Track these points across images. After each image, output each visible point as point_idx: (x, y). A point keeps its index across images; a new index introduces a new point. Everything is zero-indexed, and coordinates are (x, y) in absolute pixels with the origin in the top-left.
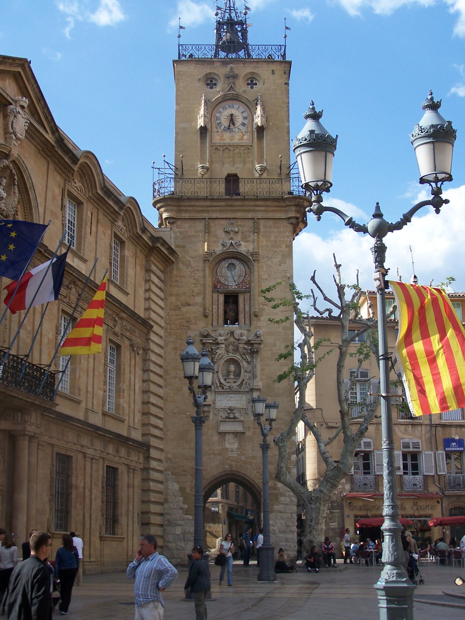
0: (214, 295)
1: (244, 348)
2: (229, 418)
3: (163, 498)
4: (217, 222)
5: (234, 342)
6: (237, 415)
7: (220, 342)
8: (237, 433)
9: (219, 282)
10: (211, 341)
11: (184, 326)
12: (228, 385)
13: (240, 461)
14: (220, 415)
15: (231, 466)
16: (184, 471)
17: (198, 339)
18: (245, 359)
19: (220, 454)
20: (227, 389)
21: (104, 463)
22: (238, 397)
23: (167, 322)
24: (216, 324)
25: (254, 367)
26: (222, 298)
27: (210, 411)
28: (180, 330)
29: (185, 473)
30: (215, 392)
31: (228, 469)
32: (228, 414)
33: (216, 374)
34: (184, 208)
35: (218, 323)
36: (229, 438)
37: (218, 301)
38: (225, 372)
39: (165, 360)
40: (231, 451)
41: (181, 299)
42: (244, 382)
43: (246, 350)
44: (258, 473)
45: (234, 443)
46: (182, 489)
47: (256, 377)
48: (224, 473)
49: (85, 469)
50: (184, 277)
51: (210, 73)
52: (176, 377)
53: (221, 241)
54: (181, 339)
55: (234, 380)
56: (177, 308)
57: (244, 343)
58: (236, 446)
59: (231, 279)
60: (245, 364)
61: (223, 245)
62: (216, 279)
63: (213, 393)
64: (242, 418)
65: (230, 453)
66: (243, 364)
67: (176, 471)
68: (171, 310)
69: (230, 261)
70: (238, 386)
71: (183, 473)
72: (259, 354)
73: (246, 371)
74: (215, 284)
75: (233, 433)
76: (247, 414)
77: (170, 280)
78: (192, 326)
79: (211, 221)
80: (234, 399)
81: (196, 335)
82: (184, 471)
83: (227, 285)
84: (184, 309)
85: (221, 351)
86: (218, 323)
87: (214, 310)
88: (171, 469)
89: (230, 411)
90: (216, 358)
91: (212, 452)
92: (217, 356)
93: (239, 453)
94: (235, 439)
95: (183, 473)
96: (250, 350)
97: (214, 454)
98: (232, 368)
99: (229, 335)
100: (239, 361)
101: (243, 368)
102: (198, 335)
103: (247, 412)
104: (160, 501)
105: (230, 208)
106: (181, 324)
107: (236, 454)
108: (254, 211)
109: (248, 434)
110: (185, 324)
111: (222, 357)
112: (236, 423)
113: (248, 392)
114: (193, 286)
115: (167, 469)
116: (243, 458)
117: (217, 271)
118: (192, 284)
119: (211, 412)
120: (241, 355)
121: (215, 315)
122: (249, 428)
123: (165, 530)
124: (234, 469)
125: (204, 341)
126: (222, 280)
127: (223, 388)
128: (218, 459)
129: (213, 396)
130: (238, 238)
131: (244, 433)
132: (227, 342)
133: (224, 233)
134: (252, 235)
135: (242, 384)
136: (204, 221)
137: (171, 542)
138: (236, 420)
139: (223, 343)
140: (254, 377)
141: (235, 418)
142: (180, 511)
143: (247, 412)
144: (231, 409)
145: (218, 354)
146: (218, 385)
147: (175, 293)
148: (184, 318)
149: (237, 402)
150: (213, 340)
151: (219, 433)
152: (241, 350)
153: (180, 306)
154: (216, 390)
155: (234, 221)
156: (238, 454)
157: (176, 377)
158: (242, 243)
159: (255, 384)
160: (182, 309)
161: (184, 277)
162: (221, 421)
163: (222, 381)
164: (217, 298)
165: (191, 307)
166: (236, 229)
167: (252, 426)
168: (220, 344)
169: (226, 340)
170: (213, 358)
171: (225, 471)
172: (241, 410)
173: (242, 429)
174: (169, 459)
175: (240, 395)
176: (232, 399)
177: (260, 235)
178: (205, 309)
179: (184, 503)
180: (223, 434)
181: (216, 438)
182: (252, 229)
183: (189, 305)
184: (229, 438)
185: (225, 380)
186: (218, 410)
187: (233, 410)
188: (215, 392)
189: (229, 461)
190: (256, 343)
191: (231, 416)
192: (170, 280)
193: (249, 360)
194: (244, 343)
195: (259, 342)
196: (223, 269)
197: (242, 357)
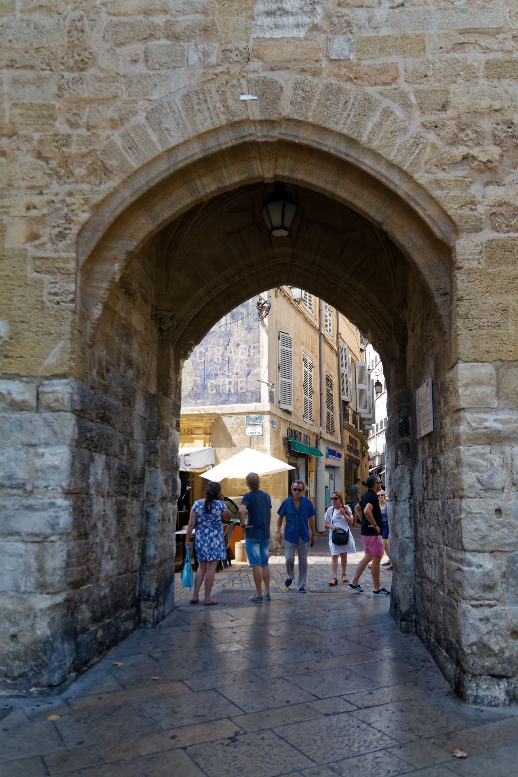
13: (324, 64)
31: (255, 114)
40: (269, 13)
65: (268, 21)
91: (159, 20)
128: (193, 58)
156: (315, 27)
171: (234, 125)
189: (255, 64)
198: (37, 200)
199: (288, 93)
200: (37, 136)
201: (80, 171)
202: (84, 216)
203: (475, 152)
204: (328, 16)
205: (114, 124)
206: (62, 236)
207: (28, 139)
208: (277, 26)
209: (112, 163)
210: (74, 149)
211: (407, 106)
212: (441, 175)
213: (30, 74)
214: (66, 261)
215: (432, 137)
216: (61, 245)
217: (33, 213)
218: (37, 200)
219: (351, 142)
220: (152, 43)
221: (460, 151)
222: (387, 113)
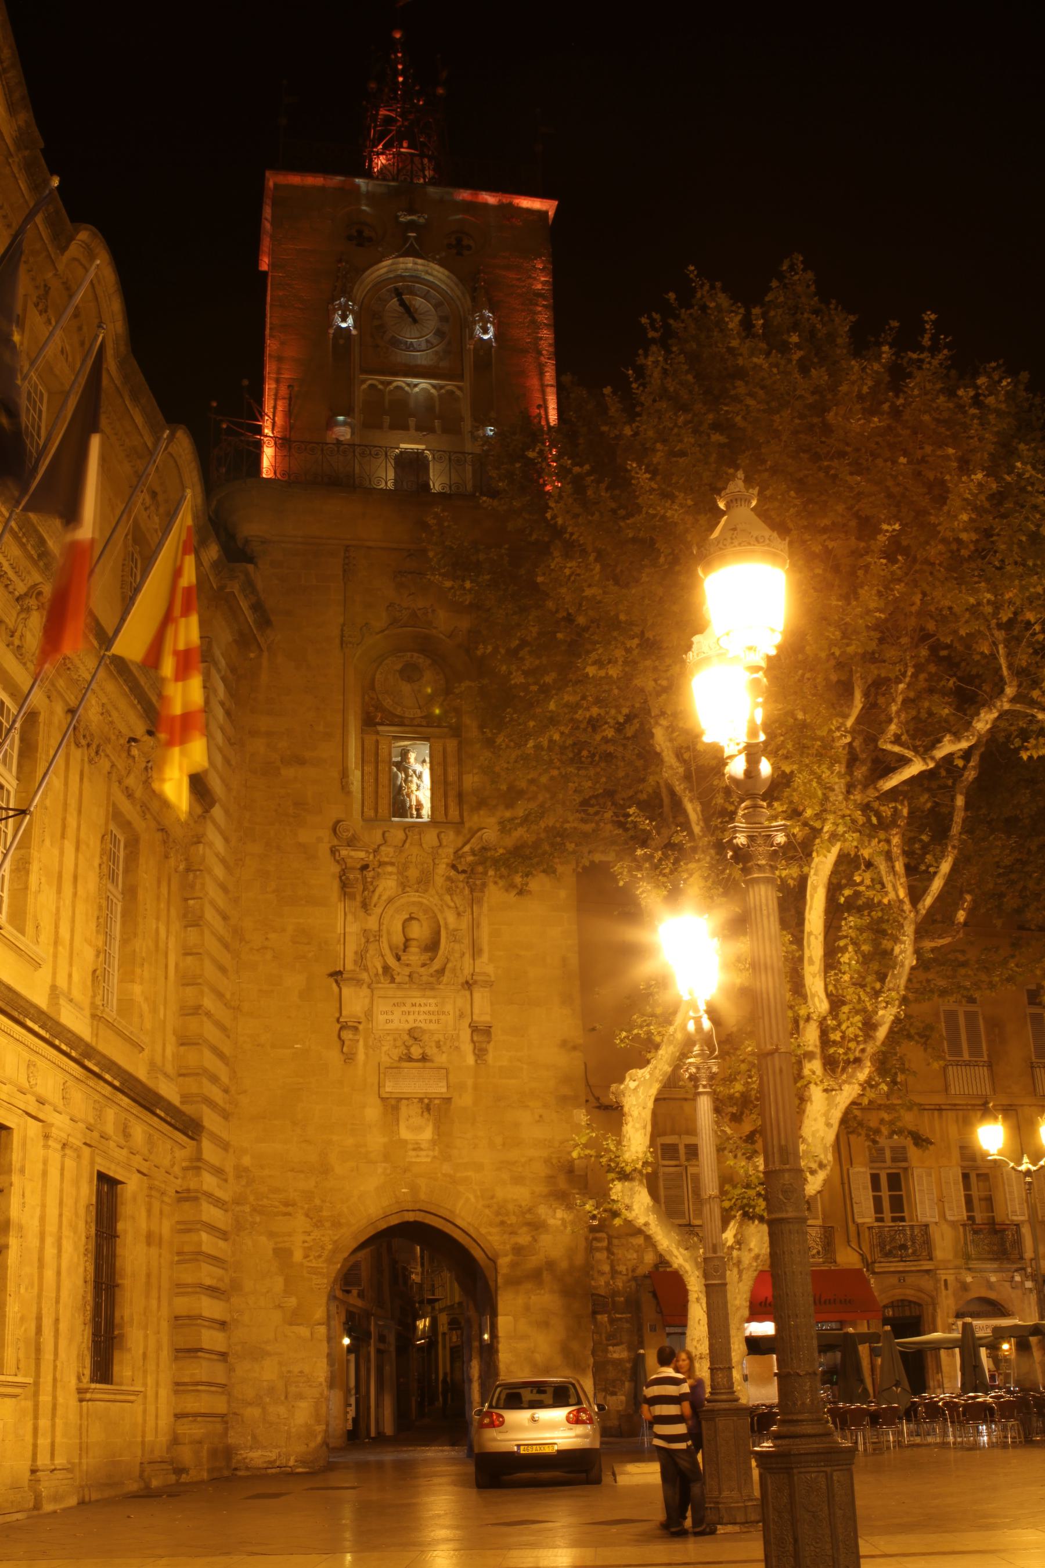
2: (410, 1059)
3: (227, 1280)
6: (432, 1051)
7: (386, 859)
15: (414, 1189)
21: (92, 1163)
24: (372, 813)
25: (475, 925)
27: (358, 1041)
29: (290, 1209)
32: (408, 1048)
35: (376, 811)
36: (410, 1114)
37: (377, 754)
38: (398, 939)
39: (236, 901)
40: (414, 1149)
42: (449, 965)
44: (489, 1206)
45: (419, 1129)
47: (480, 951)
49: (45, 1173)
52: (265, 948)
58: (427, 1134)
62: (372, 699)
66: (445, 919)
67: (265, 1202)
70: (432, 976)
72: (487, 893)
75: (421, 1100)
76: (457, 1048)
80: (422, 1009)
83: (401, 717)
84: (289, 772)
86: (376, 811)
93: (436, 1153)
101: (447, 928)
104: (221, 1285)
107: (427, 1156)
115: (238, 1201)
116: (446, 1168)
119: (361, 1043)
123: (231, 1370)
124: (423, 1196)
128: (380, 1170)
137: (250, 1404)
138: (428, 1064)
139: (392, 864)
140: (476, 951)
144: (414, 1035)
146: (380, 971)
156: (434, 1157)
157: (265, 948)
160: (283, 772)
163: (391, 961)
173: (444, 1090)
174: (246, 1170)
176: (417, 1009)
181: (373, 1112)
184: (410, 1114)
191: (416, 1052)
197: (442, 900)
198: (308, 1238)
200: (306, 1206)
201: (327, 1224)
202: (330, 1247)
203: (505, 1219)
206: (320, 1256)
207: (302, 1208)
208: (418, 1156)
209: (343, 1221)
210: (325, 1213)
214: (322, 1268)
215: (487, 1211)
216: (320, 1260)
217: (306, 1245)
218: (308, 1238)
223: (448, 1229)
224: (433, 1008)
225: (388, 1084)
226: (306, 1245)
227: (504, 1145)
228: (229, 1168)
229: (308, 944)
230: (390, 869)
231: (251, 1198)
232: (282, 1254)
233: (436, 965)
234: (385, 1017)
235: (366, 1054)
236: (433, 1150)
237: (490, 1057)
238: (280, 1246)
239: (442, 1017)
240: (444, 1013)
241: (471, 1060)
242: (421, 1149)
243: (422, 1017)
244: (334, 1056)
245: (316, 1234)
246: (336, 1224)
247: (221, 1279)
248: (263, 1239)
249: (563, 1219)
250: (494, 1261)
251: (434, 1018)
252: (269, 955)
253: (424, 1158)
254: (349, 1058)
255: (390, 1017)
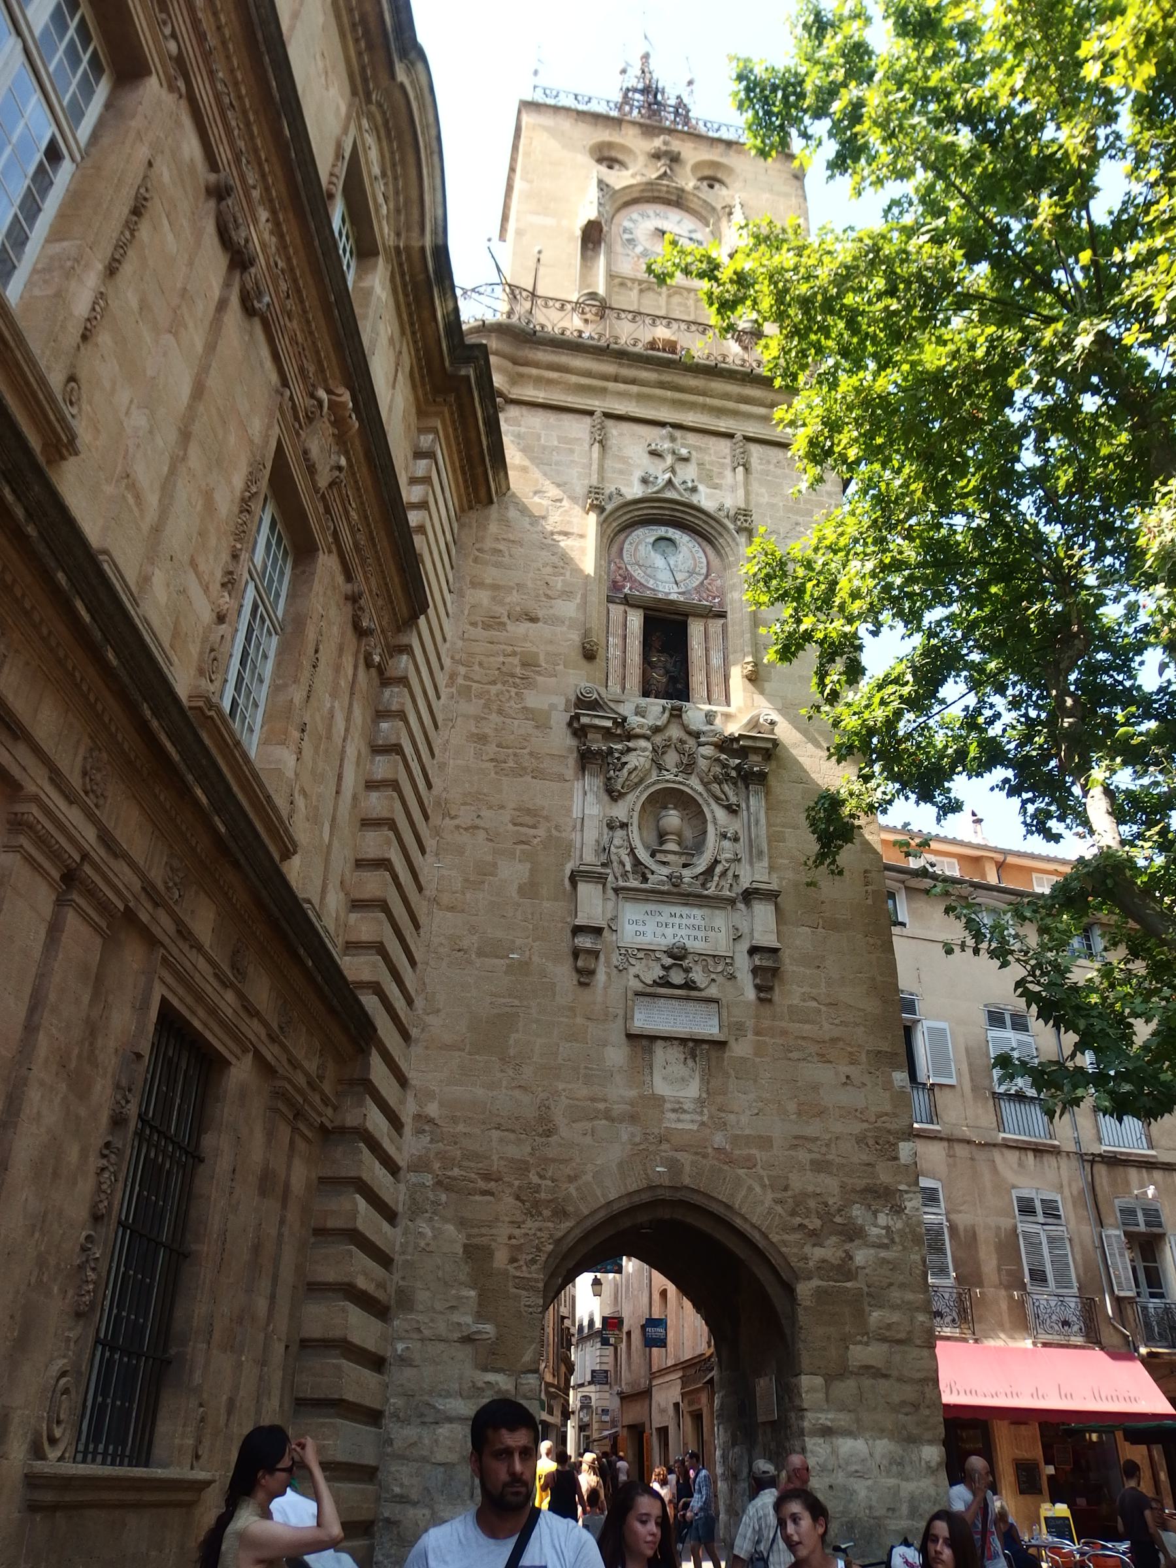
0: (611, 606)
1: (718, 760)
3: (392, 1290)
4: (626, 427)
5: (681, 741)
6: (698, 976)
7: (638, 731)
8: (698, 1042)
9: (627, 577)
10: (609, 724)
11: (513, 676)
12: (665, 871)
13: (710, 1150)
14: (632, 971)
15: (674, 1166)
16: (487, 1177)
17: (560, 719)
18: (717, 799)
19: (633, 1118)
20: (662, 883)
22: (695, 916)
23: (457, 657)
24: (619, 691)
26: (636, 620)
27: (596, 954)
28: (499, 686)
30: (616, 890)
32: (666, 968)
33: (620, 833)
34: (534, 371)
35: (623, 688)
36: (666, 1059)
38: (652, 839)
40: (674, 1111)
41: (508, 600)
42: (719, 869)
43: (725, 766)
46: (477, 1254)
47: (760, 853)
48: (646, 1197)
50: (520, 543)
51: (610, 145)
52: (477, 827)
53: (638, 474)
54: (500, 712)
55: (683, 860)
56: (493, 623)
57: (716, 745)
58: (693, 1090)
59: (665, 576)
60: (721, 814)
61: (645, 481)
63: (610, 893)
64: (713, 991)
65: (673, 1116)
67: (456, 1172)
68: (474, 624)
69: (662, 531)
71: (481, 1184)
73: (724, 836)
74: (615, 582)
75: (683, 1041)
76: (732, 977)
77: (478, 546)
78: (540, 679)
79: (610, 423)
80: (684, 921)
81: (553, 707)
82: (487, 1177)
85: (639, 758)
86: (623, 688)
87: (611, 650)
88: (437, 1165)
89: (669, 961)
90: (620, 781)
92: (625, 771)
93: (705, 1118)
94: (690, 1062)
95: (481, 1184)
96: (738, 768)
97: (608, 1116)
98: (673, 819)
99: (667, 714)
100: (701, 801)
102: (562, 707)
103: (730, 969)
104: (380, 1295)
105: (669, 394)
106: (504, 669)
108: (735, 414)
109: (740, 1049)
110: (518, 671)
111: (641, 781)
112: (691, 1006)
113: (732, 902)
114: (549, 570)
116: (719, 1139)
117: (622, 549)
118: (545, 565)
120: (705, 785)
121: (615, 664)
122: (738, 1029)
124: (687, 1181)
125: (584, 720)
126: (638, 574)
127: (645, 879)
128: (625, 1137)
129: (610, 905)
130: (688, 473)
131: (721, 1045)
132: (658, 739)
133: (647, 455)
134: (728, 473)
135: (709, 871)
136: (587, 420)
137: (415, 1504)
138: (694, 993)
139: (647, 738)
141: (689, 985)
142: (464, 1353)
143: (730, 969)
144: (678, 955)
145: (628, 767)
146: (628, 867)
147: (488, 581)
148: (514, 654)
149: (696, 933)
150: (615, 720)
151: (630, 1037)
152: (702, 764)
153: (505, 619)
154: (621, 883)
155: (678, 433)
156: (703, 1124)
158: (701, 488)
159: (757, 877)
160: (511, 627)
161: (520, 543)
162: (637, 994)
163: (643, 855)
164: (621, 619)
165: (540, 624)
166: (684, 452)
167: (750, 1023)
168: (638, 736)
169: (657, 730)
170: (609, 779)
171: (651, 1188)
172: (709, 960)
173: (715, 1031)
174: (430, 1121)
175: (706, 911)
176: (677, 921)
177: (754, 475)
178: (587, 633)
179: (480, 1317)
180: (642, 1042)
181: (617, 1055)
182: (728, 461)
183: (534, 620)
184: (666, 1059)
185: (653, 855)
186: (628, 954)
187: (682, 958)
188: (616, 890)
190: (756, 750)
191: (677, 977)
192: (478, 546)
193: (733, 799)
194: (716, 745)
195: (770, 745)
196: (641, 548)
197: (709, 791)
198: (517, 1232)
199: (687, 1168)
200: (517, 1183)
201: (547, 1213)
203: (806, 1222)
204: (711, 1117)
205: (572, 1179)
206: (533, 1261)
207: (510, 1185)
208: (679, 1120)
209: (570, 1209)
210: (543, 1195)
211: (764, 1186)
212: (786, 1237)
213: (512, 1136)
214: (536, 1280)
215: (779, 1209)
216: (534, 1267)
217: (514, 1241)
218: (517, 1232)
219: (728, 1207)
220: (596, 1122)
221: (798, 1220)
222: (750, 1189)
223: (721, 1235)
224: (697, 922)
225: (637, 1016)
226: (514, 1241)
227: (799, 1114)
228: (407, 1119)
229: (534, 827)
230: (643, 743)
231: (437, 1165)
232: (477, 1254)
233: (702, 864)
234: (634, 926)
235: (608, 975)
236: (701, 1113)
237: (776, 996)
238: (475, 1241)
239: (711, 934)
240: (713, 929)
241: (751, 994)
242: (684, 1111)
243: (683, 932)
244: (563, 974)
245: (530, 1225)
246: (560, 1213)
247: (381, 1285)
248: (450, 1228)
249: (887, 1228)
250: (790, 1290)
251: (700, 934)
252: (482, 835)
253: (687, 1124)
254: (585, 976)
255: (641, 928)
